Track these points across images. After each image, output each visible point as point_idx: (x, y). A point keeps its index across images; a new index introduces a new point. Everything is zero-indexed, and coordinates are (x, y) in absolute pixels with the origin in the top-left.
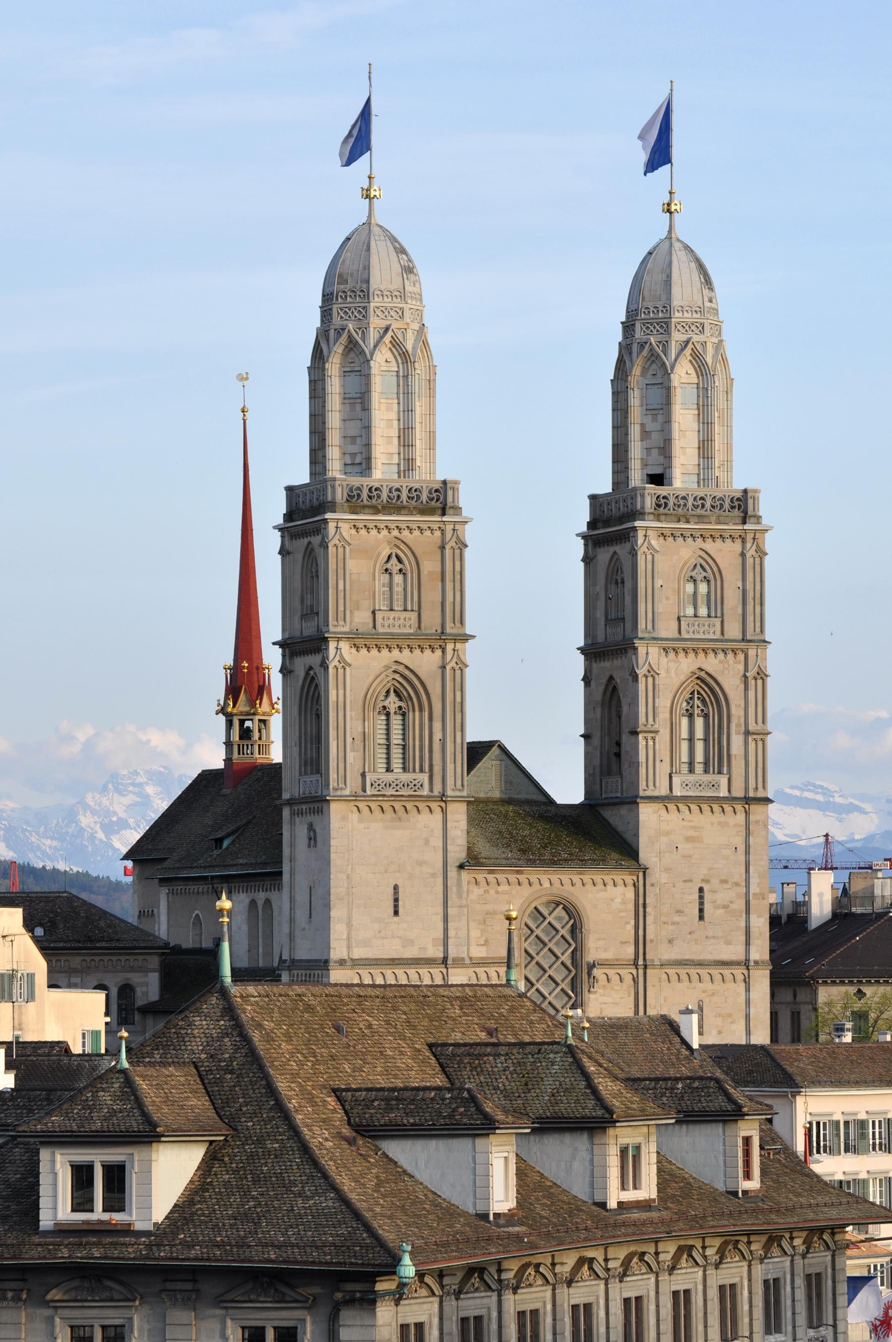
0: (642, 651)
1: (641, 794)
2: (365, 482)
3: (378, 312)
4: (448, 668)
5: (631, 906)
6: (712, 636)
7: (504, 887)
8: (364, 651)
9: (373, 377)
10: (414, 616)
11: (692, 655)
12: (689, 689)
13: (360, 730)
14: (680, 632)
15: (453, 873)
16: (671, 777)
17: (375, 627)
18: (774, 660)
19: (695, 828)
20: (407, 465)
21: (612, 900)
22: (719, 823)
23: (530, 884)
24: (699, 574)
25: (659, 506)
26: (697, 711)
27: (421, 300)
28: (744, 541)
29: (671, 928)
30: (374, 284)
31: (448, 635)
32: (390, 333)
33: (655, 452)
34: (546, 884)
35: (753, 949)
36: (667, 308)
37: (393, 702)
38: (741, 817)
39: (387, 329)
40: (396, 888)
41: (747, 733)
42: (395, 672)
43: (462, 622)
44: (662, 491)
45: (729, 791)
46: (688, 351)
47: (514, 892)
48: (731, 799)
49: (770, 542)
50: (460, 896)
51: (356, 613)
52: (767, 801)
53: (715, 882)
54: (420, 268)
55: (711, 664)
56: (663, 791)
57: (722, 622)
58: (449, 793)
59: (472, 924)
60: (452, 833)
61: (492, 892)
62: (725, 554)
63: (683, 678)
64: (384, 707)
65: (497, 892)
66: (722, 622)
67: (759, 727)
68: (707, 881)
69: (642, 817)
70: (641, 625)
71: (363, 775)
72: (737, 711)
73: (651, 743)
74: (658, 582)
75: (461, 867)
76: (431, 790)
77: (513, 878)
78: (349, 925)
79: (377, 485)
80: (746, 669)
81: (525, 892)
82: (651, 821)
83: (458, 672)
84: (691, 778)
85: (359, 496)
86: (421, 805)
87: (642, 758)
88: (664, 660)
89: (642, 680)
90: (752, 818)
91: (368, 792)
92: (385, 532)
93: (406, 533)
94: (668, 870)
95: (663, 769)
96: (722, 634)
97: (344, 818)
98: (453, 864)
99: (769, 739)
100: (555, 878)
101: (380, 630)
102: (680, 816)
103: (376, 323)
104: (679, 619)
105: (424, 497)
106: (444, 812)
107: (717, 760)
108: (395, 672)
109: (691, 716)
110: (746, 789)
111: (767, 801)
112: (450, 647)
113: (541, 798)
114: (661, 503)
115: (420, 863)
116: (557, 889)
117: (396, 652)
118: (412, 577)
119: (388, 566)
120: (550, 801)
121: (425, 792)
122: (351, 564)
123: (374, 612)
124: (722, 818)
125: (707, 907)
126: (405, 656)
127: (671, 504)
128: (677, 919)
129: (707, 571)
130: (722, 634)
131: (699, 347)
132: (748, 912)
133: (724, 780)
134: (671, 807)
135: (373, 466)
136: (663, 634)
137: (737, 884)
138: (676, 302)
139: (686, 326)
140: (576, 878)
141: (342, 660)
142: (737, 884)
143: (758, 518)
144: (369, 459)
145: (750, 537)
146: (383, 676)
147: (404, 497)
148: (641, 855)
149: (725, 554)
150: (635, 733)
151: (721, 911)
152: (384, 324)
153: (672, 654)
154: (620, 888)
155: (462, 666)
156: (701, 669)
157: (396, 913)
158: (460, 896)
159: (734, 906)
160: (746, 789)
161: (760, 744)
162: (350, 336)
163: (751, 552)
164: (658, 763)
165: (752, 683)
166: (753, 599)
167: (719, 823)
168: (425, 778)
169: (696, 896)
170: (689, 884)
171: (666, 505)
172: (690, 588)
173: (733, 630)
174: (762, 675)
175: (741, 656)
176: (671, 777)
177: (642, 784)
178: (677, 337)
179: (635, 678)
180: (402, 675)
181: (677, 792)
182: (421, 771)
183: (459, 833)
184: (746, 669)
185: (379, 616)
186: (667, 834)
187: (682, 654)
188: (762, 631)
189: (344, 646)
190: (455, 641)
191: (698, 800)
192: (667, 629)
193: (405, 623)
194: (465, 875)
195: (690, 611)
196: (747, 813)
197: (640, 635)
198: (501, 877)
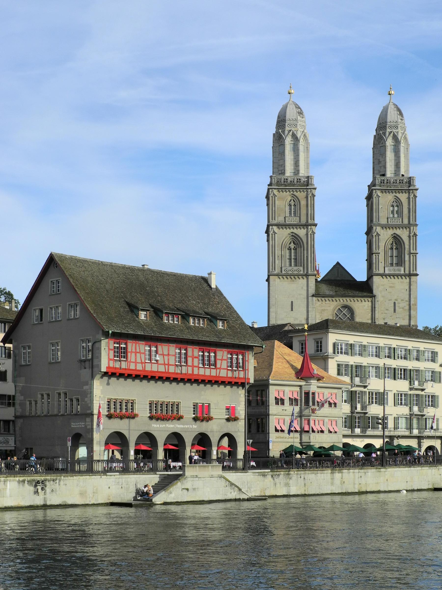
0: (374, 228)
1: (374, 272)
2: (283, 177)
3: (289, 126)
4: (309, 234)
5: (370, 308)
6: (399, 223)
7: (328, 302)
8: (281, 229)
9: (286, 145)
10: (298, 218)
11: (391, 229)
12: (392, 240)
13: (280, 253)
14: (388, 222)
15: (310, 298)
16: (384, 268)
17: (285, 222)
18: (419, 230)
19: (393, 284)
20: (297, 171)
21: (364, 306)
22: (401, 282)
23: (336, 301)
24: (395, 204)
25: (381, 183)
26: (394, 247)
27: (305, 123)
28: (409, 193)
29: (384, 315)
30: (287, 117)
31: (309, 225)
32: (291, 132)
33: (382, 167)
34: (342, 301)
35: (412, 321)
36: (386, 122)
37: (292, 246)
38: (408, 280)
39: (291, 130)
40: (292, 302)
41: (410, 253)
42: (292, 236)
43: (314, 220)
44: (383, 178)
45: (404, 272)
46: (392, 135)
47: (331, 303)
48: (405, 275)
49: (418, 193)
50: (313, 304)
51: (279, 217)
52: (417, 275)
53: (399, 301)
54: (305, 113)
55: (398, 232)
56: (381, 271)
57: (402, 219)
58: (309, 272)
59: (317, 314)
60: (310, 285)
61: (324, 303)
62: (403, 197)
63: (389, 236)
64: (289, 247)
65: (326, 304)
66: (402, 219)
67: (414, 251)
68: (396, 300)
69: (374, 280)
70: (374, 220)
71: (281, 268)
72: (407, 247)
73: (377, 257)
74: (380, 207)
75: (313, 296)
76: (304, 272)
77: (330, 299)
78: (276, 313)
79: (286, 178)
80: (410, 233)
81: (335, 303)
82: (376, 280)
83: (312, 235)
84: (392, 268)
85: (281, 181)
86: (300, 277)
87: (374, 261)
88: (382, 231)
89: (374, 237)
90: (412, 280)
91: (283, 273)
92: (288, 192)
93: (295, 192)
94: (383, 297)
95: (381, 265)
96: (402, 222)
97: (274, 280)
98: (310, 294)
99: (417, 255)
100: (344, 299)
101: (287, 222)
102: (388, 280)
103: (287, 129)
104: (388, 218)
105: (302, 182)
106: (308, 279)
107: (400, 263)
108: (292, 236)
109: (392, 249)
110: (410, 271)
111: (417, 275)
112: (309, 227)
113: (352, 279)
114: (382, 182)
115: (300, 295)
116: (345, 303)
117: (292, 229)
118: (298, 207)
119: (290, 203)
120: (355, 280)
121: (302, 272)
122: (277, 202)
123: (285, 218)
124: (402, 280)
125: (397, 308)
126: (295, 231)
127: (385, 182)
128: (386, 312)
129: (398, 203)
130: (402, 222)
131: (396, 134)
132: (410, 309)
133: (402, 269)
134: (384, 277)
135: (286, 172)
136: (382, 223)
137: (407, 301)
138: (388, 120)
139: (391, 127)
140: (352, 299)
141: (274, 232)
142: (407, 301)
143: (414, 186)
144: (285, 170)
145: (411, 191)
146: (288, 237)
147: (295, 181)
148: (374, 292)
149: (403, 197)
150: (373, 254)
151: (401, 309)
152: (290, 129)
153: (385, 229)
154: (367, 302)
155: (314, 233)
156: (395, 234)
157: (292, 310)
158: (313, 304)
159: (405, 308)
160: (410, 271)
161: (414, 257)
162: (280, 134)
163: (412, 196)
164: (380, 263)
165: (412, 238)
166: (412, 211)
167: (401, 282)
168: (302, 268)
169: (393, 305)
170: (390, 301)
171: (384, 182)
172: (391, 208)
173: (406, 221)
174: (415, 235)
175: (408, 229)
176: (384, 268)
177: (374, 270)
178: (388, 130)
179: (373, 236)
180: (295, 237)
181: (387, 272)
182: (301, 266)
183: (312, 285)
184: (410, 233)
185: (287, 219)
186: (383, 285)
187: (388, 229)
188: (415, 221)
189: (275, 228)
190: (311, 225)
191: (394, 275)
192: (383, 221)
193: (294, 220)
194: (314, 298)
195: (391, 216)
196: (410, 279)
197: (374, 223)
198: (327, 299)
